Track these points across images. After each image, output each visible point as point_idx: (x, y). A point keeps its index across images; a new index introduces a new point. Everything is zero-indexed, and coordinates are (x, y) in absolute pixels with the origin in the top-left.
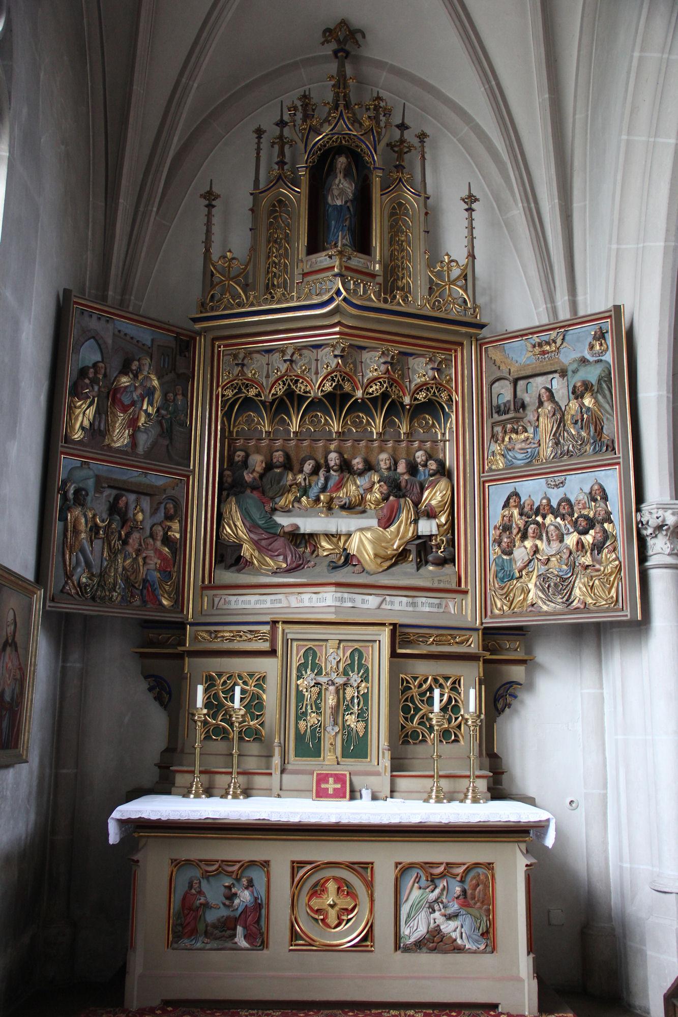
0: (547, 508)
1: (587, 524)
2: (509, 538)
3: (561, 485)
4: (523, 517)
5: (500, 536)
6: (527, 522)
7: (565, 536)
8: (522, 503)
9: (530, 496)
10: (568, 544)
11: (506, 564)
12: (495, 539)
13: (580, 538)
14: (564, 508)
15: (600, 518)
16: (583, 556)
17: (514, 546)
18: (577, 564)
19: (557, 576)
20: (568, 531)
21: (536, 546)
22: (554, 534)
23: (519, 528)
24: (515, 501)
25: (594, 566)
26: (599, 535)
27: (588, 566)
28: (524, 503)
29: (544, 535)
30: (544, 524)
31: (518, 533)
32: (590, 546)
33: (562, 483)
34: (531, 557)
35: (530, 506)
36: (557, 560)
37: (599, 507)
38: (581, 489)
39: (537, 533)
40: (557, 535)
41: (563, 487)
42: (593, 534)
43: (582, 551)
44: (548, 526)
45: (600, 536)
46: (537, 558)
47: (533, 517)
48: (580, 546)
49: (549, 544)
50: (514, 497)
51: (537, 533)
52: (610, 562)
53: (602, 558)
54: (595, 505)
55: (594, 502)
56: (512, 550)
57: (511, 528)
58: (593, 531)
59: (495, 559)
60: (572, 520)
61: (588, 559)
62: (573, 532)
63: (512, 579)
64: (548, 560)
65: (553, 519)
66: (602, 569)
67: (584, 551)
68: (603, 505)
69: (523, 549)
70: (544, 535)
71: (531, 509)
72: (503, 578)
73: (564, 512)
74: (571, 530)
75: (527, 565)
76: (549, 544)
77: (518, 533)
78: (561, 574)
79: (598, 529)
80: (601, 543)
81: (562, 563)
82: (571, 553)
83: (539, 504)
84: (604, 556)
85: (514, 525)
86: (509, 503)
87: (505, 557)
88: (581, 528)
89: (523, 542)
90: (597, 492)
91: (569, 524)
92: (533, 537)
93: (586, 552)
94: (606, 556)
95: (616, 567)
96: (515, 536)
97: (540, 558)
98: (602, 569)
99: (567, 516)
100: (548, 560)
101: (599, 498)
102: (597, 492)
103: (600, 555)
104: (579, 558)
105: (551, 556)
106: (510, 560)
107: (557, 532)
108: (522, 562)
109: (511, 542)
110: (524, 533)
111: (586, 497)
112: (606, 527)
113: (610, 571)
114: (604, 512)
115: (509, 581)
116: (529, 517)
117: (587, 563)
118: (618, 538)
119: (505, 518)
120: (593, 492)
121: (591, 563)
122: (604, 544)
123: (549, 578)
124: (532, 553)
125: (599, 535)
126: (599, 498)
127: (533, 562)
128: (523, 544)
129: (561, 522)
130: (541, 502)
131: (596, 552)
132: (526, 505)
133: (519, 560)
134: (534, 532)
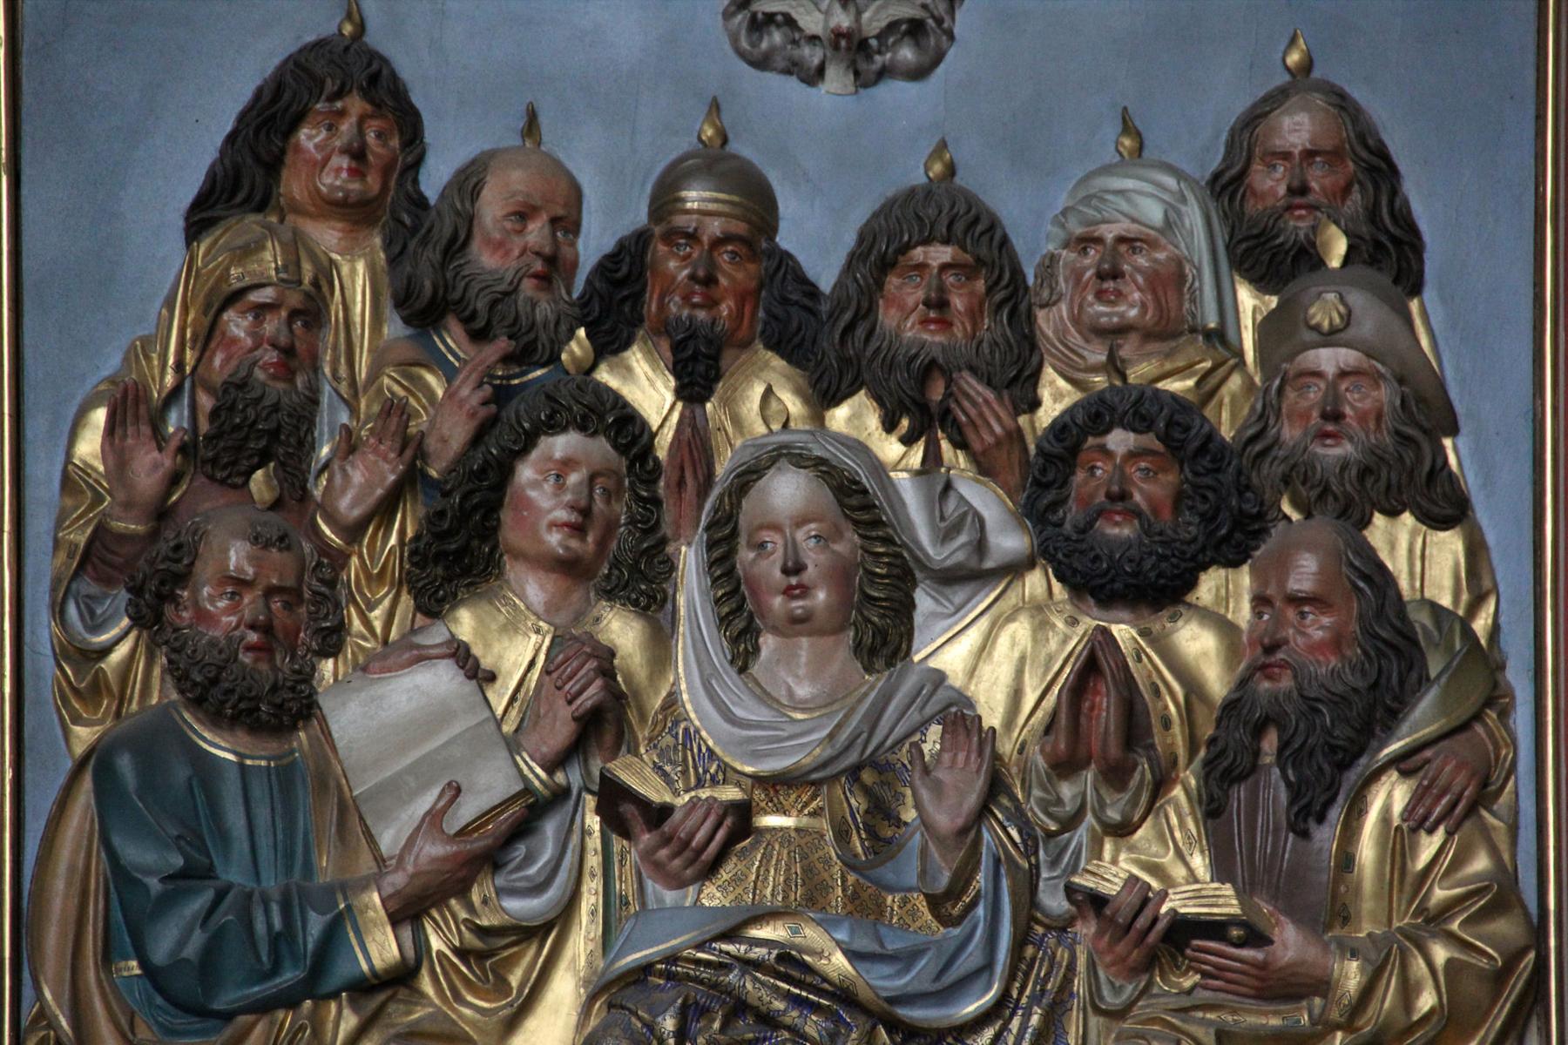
0: (732, 273)
1: (1179, 499)
2: (283, 541)
3: (907, 54)
4: (452, 340)
5: (162, 513)
6: (502, 395)
7: (924, 601)
8: (434, 178)
9: (531, 125)
10: (956, 679)
11: (235, 819)
12: (101, 532)
13: (1106, 632)
14: (939, 303)
15: (1345, 449)
16: (1123, 830)
17: (332, 641)
18: (1054, 901)
19: (844, 995)
20: (980, 546)
21: (605, 659)
22: (814, 559)
23: (414, 450)
24: (358, 154)
25: (1256, 937)
26: (1318, 626)
27: (1184, 931)
28: (469, 181)
29: (689, 559)
30: (695, 441)
31: (384, 510)
32: (1207, 730)
33: (915, 30)
34: (537, 774)
35: (536, 233)
36: (842, 836)
37: (1330, 337)
38: (1128, 127)
39: (610, 527)
40: (841, 575)
41: (919, 73)
42: (1243, 613)
43: (1116, 775)
44: (748, 476)
45: (1336, 642)
46: (614, 799)
47: (578, 345)
48: (1105, 707)
49: (743, 658)
50: (356, 105)
51: (610, 527)
52: (1435, 920)
53: (1347, 860)
54: (1268, 328)
55: (1262, 283)
56: (306, 676)
57: (306, 446)
58: (1244, 578)
59: (99, 760)
60: (1017, 436)
61: (1179, 872)
62: (1014, 570)
63: (314, 986)
64: (741, 819)
65: (793, 404)
66: (1352, 975)
67: (1144, 771)
68: (1370, 314)
69: (441, 679)
70: (689, 559)
71: (554, 266)
72: (209, 965)
73: (934, 338)
74: (1009, 541)
75: (491, 859)
76: (743, 658)
77: (384, 510)
78: (882, 981)
79: (1305, 573)
80: (1340, 702)
81: (910, 871)
82: (996, 786)
83: (638, 216)
84: (1367, 850)
85: (332, 417)
86: (273, 166)
87: (221, 748)
88: (1120, 531)
89: (434, 605)
90: (1318, 179)
91: (984, 467)
92: (569, 568)
93: (1161, 785)
94: (1398, 842)
95: (1500, 977)
96: (353, 532)
97: (654, 791)
98: (1352, 975)
99: (971, 384)
100: (741, 819)
101: (1337, 249)
102: (1318, 179)
103: (1326, 836)
104: (1082, 834)
105: (777, 785)
106: (284, 777)
107: (848, 544)
108: (435, 817)
109: (292, 596)
110: (464, 515)
111: (1193, 216)
112: (1398, 564)
113: (1426, 1001)
114: (1385, 395)
115: (263, 1007)
116: (522, 357)
117: (1178, 903)
118: (1517, 677)
119: (237, 325)
120: (1271, 183)
121: (1226, 902)
122: (1391, 716)
123: (739, 1007)
124: (560, 731)
125: (1318, 626)
126: (1337, 249)
127: (550, 828)
128: (435, 636)
129: (890, 449)
130: (664, 199)
131: (1276, 791)
132: (492, 208)
133: (395, 791)
134: (586, 512)
